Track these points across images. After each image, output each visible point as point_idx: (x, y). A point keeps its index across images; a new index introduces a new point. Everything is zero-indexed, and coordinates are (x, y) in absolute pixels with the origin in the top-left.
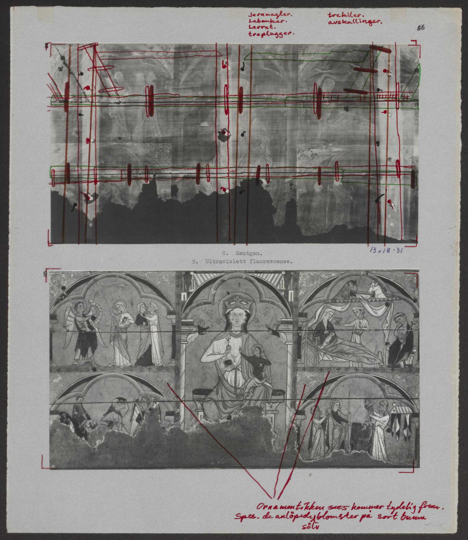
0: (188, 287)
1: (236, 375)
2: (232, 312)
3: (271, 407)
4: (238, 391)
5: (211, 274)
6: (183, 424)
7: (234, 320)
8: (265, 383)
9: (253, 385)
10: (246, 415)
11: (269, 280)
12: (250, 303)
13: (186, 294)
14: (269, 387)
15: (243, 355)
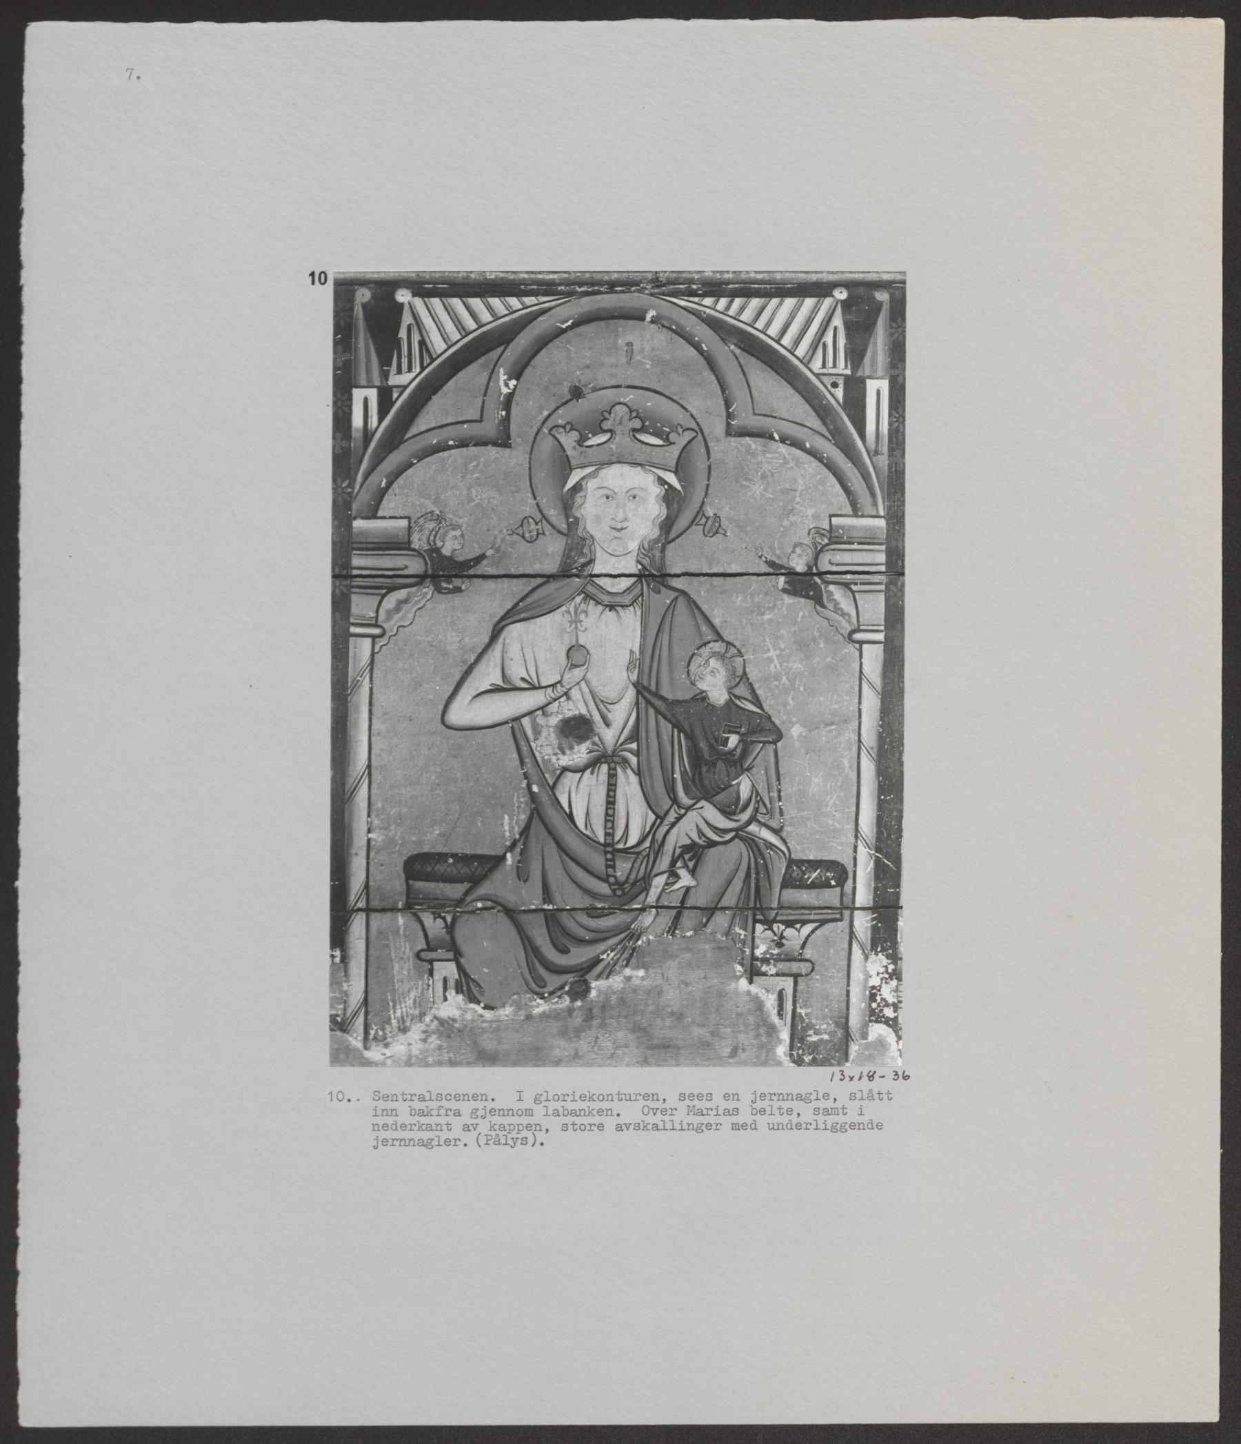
0: (385, 362)
1: (612, 787)
2: (591, 485)
3: (780, 945)
4: (622, 869)
5: (495, 302)
6: (360, 1020)
7: (606, 525)
8: (753, 828)
9: (695, 836)
10: (659, 982)
11: (773, 331)
12: (681, 440)
13: (372, 394)
14: (771, 846)
15: (645, 692)
